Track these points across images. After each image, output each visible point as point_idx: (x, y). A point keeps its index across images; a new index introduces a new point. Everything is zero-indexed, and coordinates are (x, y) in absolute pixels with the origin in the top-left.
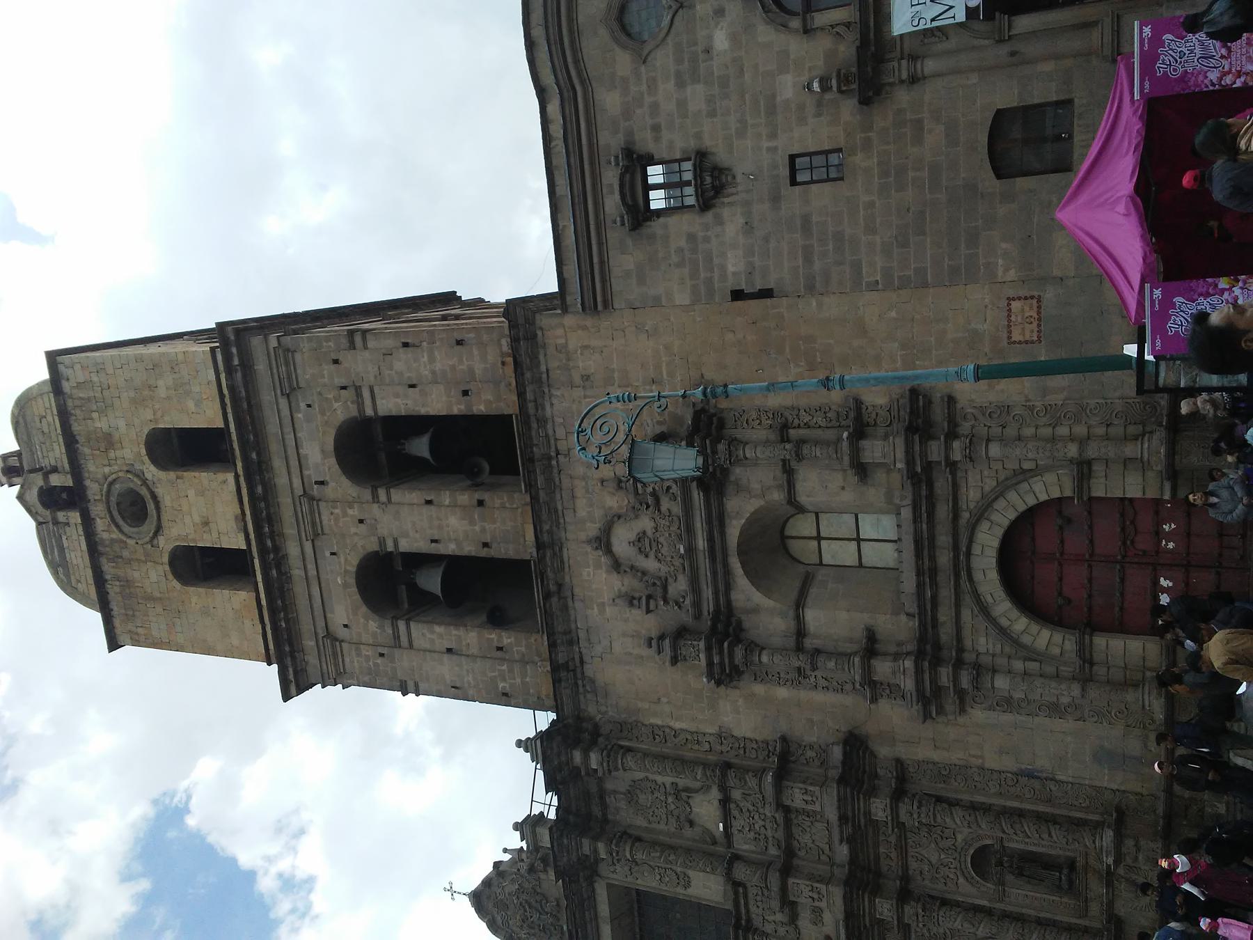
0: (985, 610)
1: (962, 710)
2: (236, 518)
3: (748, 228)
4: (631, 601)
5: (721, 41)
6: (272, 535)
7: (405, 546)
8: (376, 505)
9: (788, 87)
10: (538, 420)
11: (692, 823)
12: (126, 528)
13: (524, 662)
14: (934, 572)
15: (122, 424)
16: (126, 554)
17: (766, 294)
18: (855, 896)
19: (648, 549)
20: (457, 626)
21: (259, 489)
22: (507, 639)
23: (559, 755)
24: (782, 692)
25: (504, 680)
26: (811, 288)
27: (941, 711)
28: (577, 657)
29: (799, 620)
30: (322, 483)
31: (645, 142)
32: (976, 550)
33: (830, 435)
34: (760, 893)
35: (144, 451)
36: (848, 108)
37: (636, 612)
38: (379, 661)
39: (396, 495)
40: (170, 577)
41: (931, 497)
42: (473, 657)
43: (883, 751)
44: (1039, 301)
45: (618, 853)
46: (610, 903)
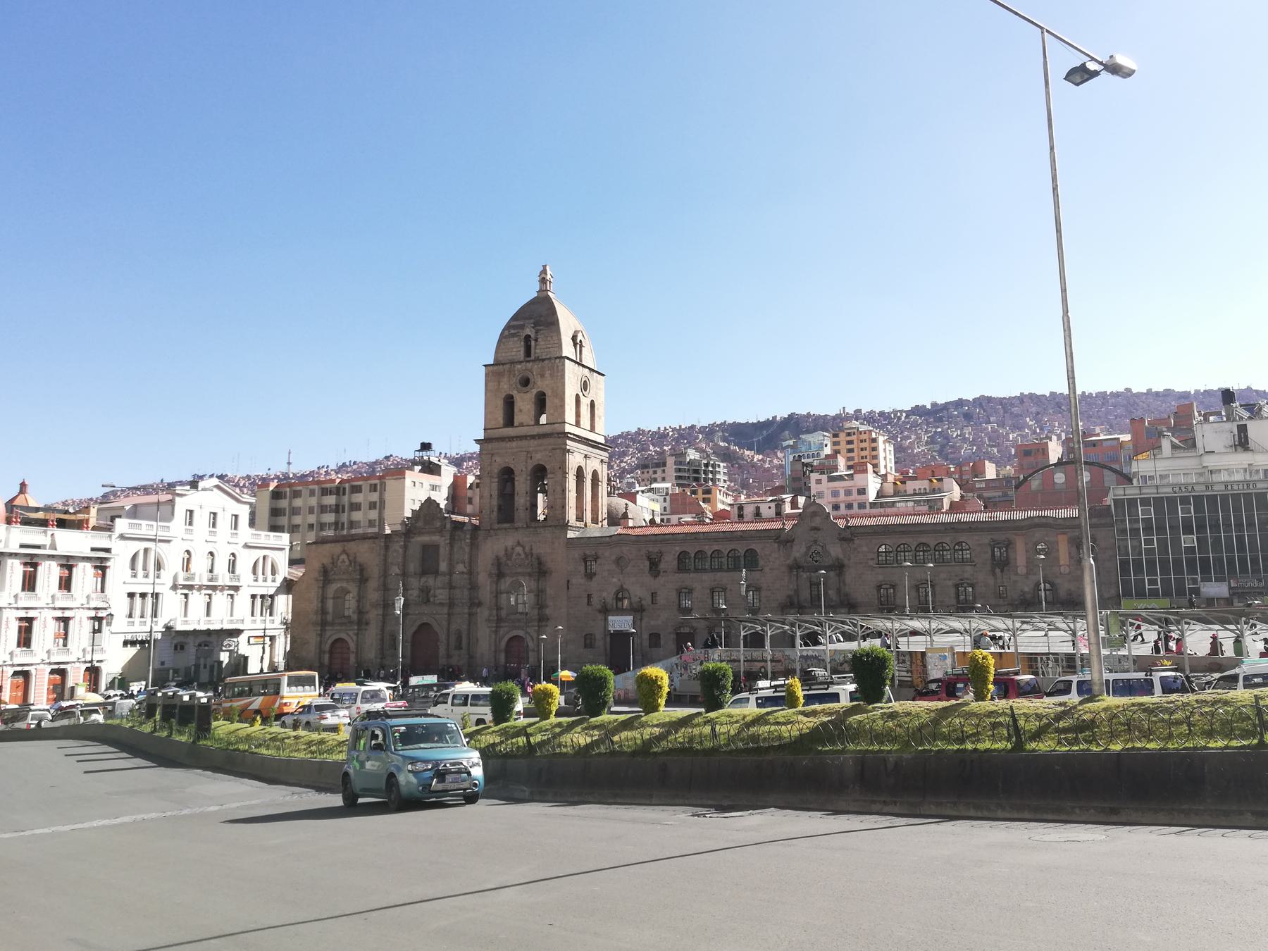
0: (507, 633)
2: (522, 423)
4: (506, 550)
5: (615, 580)
7: (516, 483)
8: (525, 476)
9: (605, 594)
11: (458, 563)
12: (519, 378)
13: (490, 518)
15: (547, 382)
16: (511, 376)
17: (568, 588)
20: (498, 499)
22: (495, 513)
29: (504, 593)
30: (531, 457)
31: (599, 561)
33: (540, 602)
35: (540, 390)
36: (599, 607)
37: (503, 552)
38: (487, 472)
39: (528, 482)
40: (506, 394)
42: (490, 503)
43: (479, 610)
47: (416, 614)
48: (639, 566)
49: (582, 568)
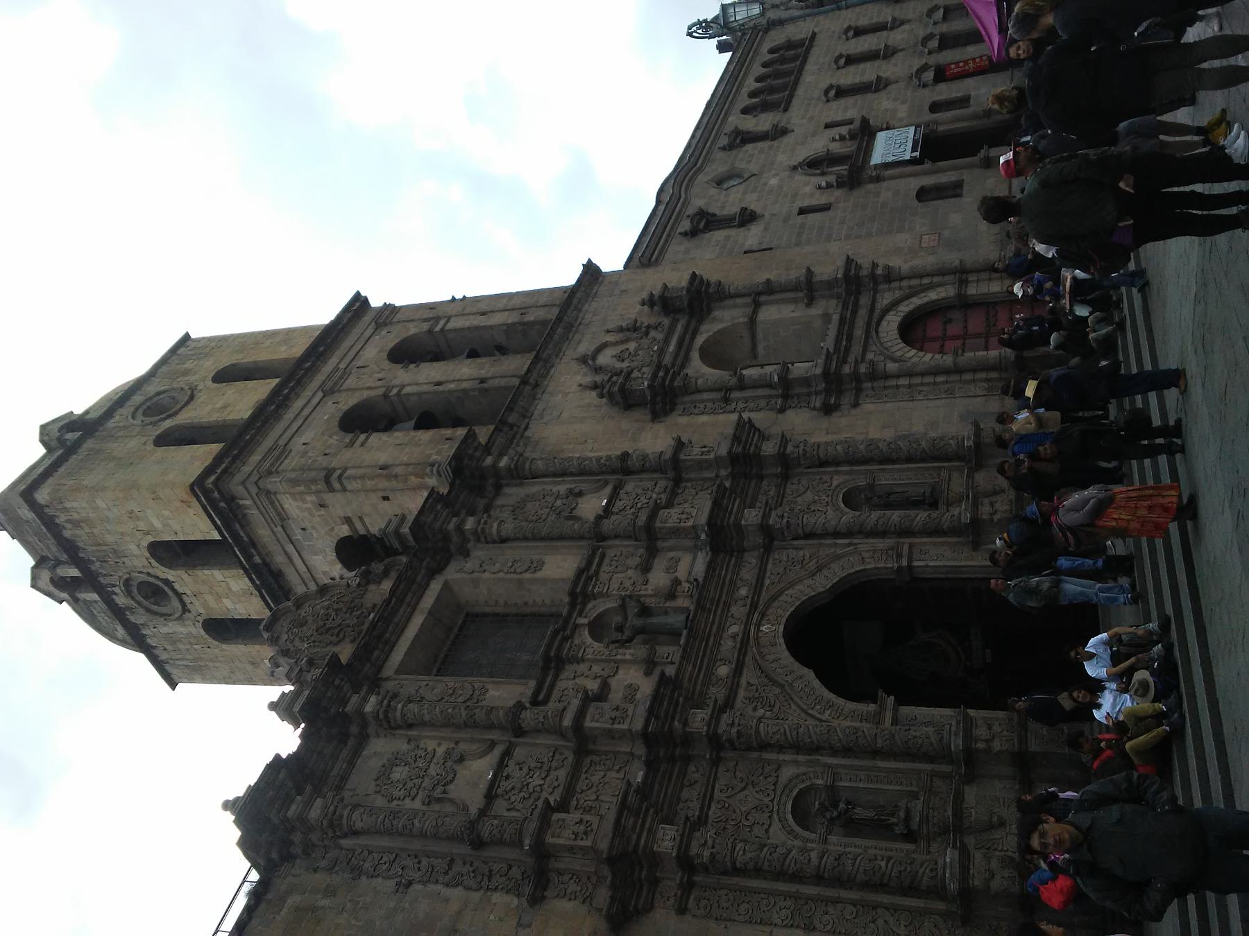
1: (856, 405)
3: (766, 229)
6: (293, 389)
10: (576, 307)
14: (850, 338)
18: (727, 494)
19: (626, 356)
21: (308, 365)
23: (476, 449)
24: (704, 418)
25: (439, 453)
26: (798, 244)
27: (837, 407)
28: (523, 426)
32: (884, 323)
34: (619, 554)
41: (856, 303)
44: (939, 237)
45: (485, 523)
46: (438, 599)
47: (738, 671)
48: (752, 156)
49: (719, 235)
